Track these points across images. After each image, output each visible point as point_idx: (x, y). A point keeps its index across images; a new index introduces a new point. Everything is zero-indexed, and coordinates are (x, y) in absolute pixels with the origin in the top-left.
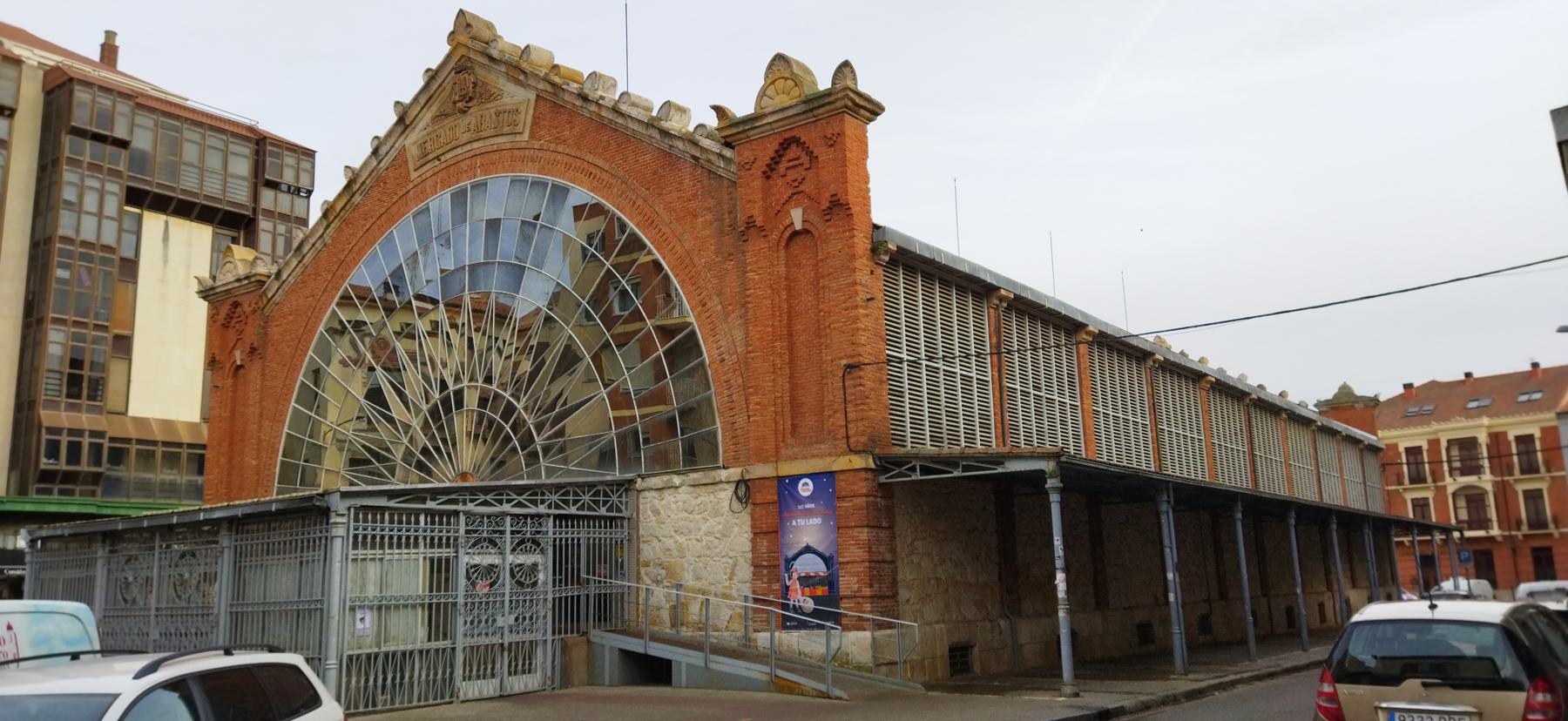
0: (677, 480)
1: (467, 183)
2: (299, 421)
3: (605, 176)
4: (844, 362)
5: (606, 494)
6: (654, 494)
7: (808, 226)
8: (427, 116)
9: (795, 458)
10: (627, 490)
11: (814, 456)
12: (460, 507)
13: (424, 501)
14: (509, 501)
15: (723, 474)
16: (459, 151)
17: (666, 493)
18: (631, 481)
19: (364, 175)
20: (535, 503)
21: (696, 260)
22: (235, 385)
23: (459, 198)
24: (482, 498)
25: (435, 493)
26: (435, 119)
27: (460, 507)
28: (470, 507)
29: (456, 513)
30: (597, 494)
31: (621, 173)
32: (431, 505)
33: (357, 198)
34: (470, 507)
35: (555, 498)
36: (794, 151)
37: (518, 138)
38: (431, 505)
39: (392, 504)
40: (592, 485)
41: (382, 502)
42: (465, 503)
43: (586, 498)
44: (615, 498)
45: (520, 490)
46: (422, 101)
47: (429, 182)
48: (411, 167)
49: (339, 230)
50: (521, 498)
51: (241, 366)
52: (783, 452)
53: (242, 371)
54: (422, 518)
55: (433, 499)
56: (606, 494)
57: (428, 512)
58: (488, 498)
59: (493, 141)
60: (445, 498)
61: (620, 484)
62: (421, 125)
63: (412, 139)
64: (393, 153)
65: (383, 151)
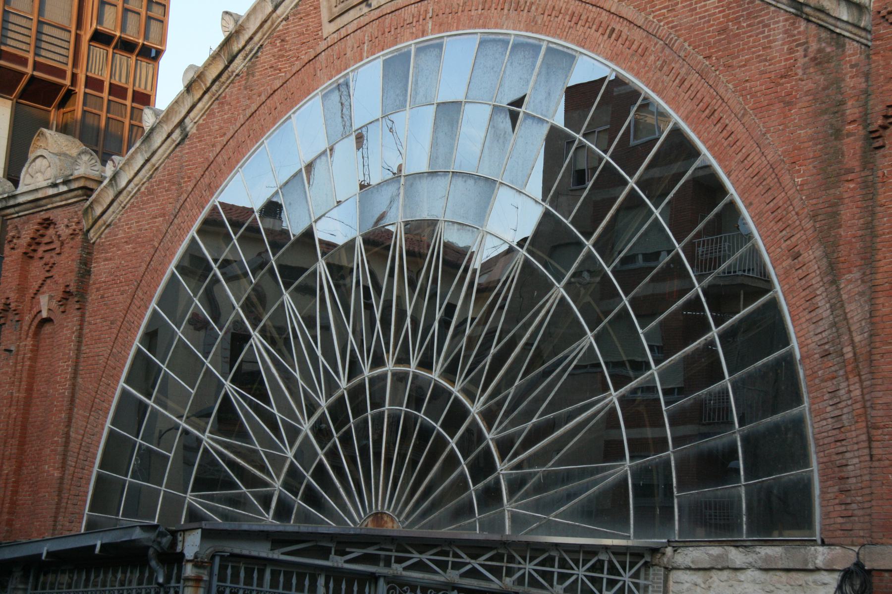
0: (736, 556)
1: (410, 44)
2: (131, 412)
3: (637, 35)
5: (613, 570)
6: (698, 577)
10: (647, 565)
12: (378, 569)
13: (325, 553)
14: (456, 566)
15: (821, 555)
17: (715, 575)
18: (654, 551)
19: (252, 27)
20: (496, 571)
21: (786, 179)
22: (35, 350)
23: (396, 71)
24: (416, 557)
25: (343, 542)
27: (378, 569)
28: (397, 569)
29: (374, 578)
30: (598, 567)
31: (664, 30)
32: (336, 561)
33: (239, 64)
34: (397, 569)
35: (529, 567)
38: (336, 561)
39: (277, 555)
40: (591, 551)
41: (262, 550)
42: (388, 564)
43: (581, 572)
44: (626, 577)
45: (475, 548)
47: (350, 41)
48: (325, 16)
49: (209, 113)
50: (475, 564)
51: (48, 320)
53: (48, 328)
54: (321, 581)
55: (341, 553)
56: (613, 570)
57: (333, 574)
58: (425, 557)
60: (357, 553)
61: (636, 554)
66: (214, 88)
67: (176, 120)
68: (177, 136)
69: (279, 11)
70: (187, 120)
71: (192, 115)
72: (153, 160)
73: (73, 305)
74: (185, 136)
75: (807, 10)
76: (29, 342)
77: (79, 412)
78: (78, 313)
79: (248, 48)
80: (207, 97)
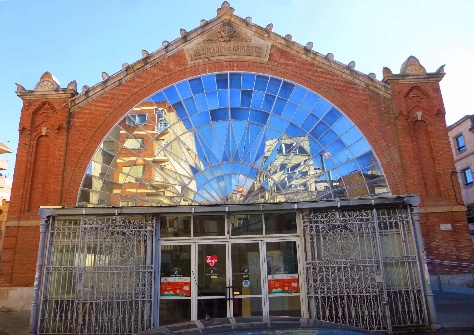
4: (450, 171)
7: (423, 119)
8: (200, 39)
9: (431, 206)
11: (442, 206)
16: (223, 57)
26: (205, 42)
33: (148, 66)
36: (415, 91)
37: (262, 59)
46: (199, 32)
49: (133, 79)
52: (425, 203)
59: (244, 57)
62: (195, 42)
63: (188, 47)
64: (175, 51)
65: (170, 48)
66: (136, 72)
67: (119, 78)
68: (117, 83)
69: (167, 54)
70: (123, 79)
71: (125, 78)
72: (106, 89)
73: (64, 131)
74: (120, 84)
75: (371, 87)
76: (35, 142)
77: (68, 168)
78: (66, 134)
79: (153, 62)
80: (133, 73)
